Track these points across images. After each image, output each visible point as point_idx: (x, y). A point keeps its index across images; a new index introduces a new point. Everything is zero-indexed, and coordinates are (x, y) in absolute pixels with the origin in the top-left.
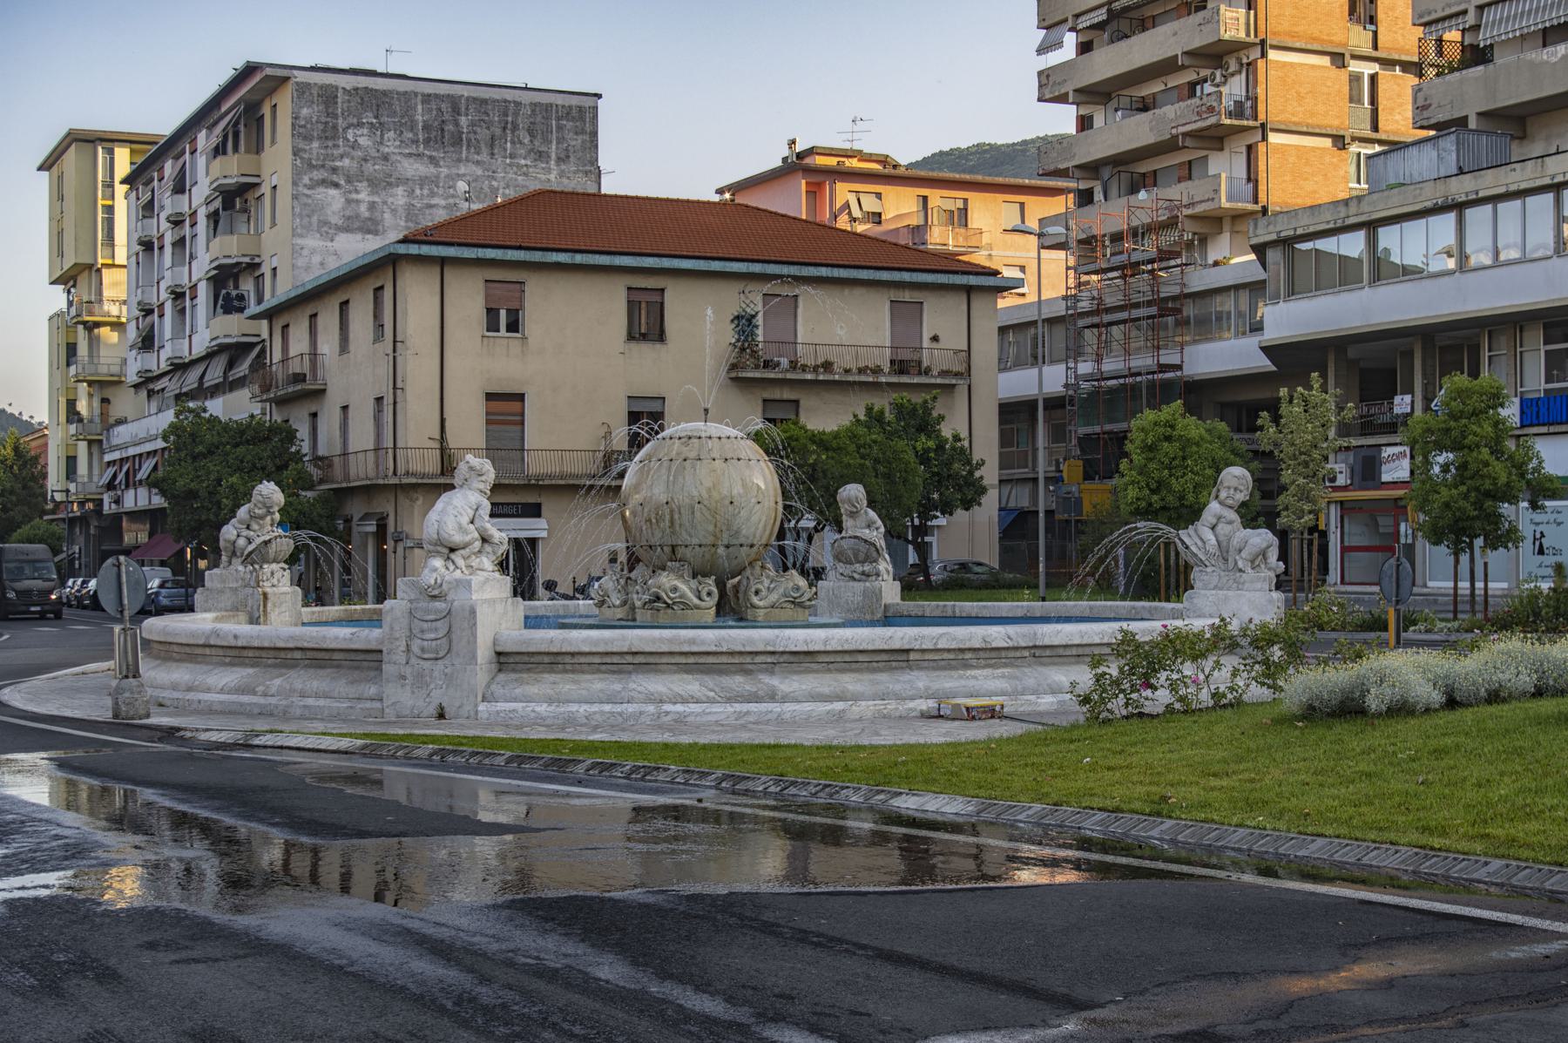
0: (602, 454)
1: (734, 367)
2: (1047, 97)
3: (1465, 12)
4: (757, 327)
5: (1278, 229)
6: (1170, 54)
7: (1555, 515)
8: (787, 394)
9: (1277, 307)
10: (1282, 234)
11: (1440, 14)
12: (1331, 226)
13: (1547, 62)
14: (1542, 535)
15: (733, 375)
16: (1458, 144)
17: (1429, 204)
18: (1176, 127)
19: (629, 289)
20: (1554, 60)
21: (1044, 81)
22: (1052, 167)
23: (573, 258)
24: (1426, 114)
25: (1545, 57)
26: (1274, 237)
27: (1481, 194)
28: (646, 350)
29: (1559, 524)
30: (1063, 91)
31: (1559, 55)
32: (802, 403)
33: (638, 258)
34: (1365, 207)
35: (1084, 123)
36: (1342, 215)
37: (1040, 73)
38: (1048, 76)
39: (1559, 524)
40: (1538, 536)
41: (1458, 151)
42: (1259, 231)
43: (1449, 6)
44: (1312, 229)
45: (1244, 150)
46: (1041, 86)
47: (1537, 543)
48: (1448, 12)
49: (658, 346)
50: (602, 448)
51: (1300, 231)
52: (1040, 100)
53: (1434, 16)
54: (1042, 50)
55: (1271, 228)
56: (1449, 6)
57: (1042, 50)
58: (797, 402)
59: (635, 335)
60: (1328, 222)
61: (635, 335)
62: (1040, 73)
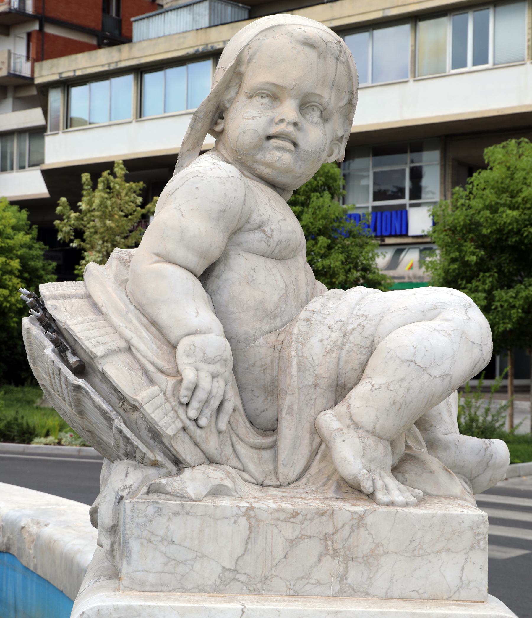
5: (60, 70)
10: (65, 75)
12: (106, 68)
16: (210, 9)
17: (191, 51)
26: (56, 77)
36: (116, 59)
45: (25, 36)
51: (78, 73)
55: (54, 70)
60: (103, 65)
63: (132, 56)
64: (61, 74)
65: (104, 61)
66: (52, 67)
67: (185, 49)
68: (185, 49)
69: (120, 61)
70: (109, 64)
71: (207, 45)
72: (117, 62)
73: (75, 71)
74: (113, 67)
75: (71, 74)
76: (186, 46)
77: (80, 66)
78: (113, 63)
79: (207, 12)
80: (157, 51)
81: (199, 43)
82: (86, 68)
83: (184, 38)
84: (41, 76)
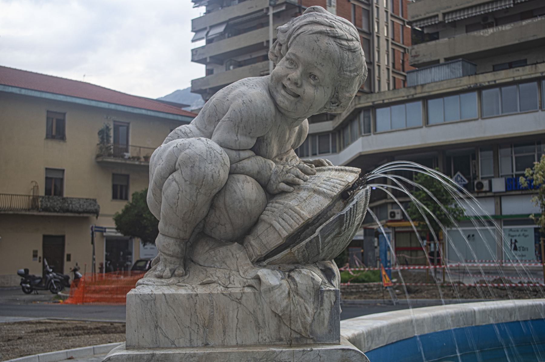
0: (31, 198)
1: (98, 156)
2: (196, 59)
3: (437, 16)
4: (110, 137)
5: (373, 100)
6: (260, 41)
7: (523, 232)
8: (124, 172)
9: (370, 137)
10: (376, 103)
11: (423, 17)
12: (406, 98)
13: (483, 36)
14: (516, 241)
15: (100, 160)
18: (263, 72)
19: (48, 112)
20: (487, 35)
21: (194, 53)
22: (198, 88)
23: (20, 91)
24: (416, 59)
25: (482, 34)
27: (497, 82)
28: (55, 145)
29: (526, 236)
30: (204, 57)
31: (489, 33)
32: (131, 176)
33: (55, 95)
34: (426, 89)
35: (209, 72)
37: (192, 50)
38: (196, 51)
39: (526, 236)
40: (513, 241)
41: (463, 69)
42: (362, 101)
43: (428, 13)
44: (393, 100)
46: (193, 55)
47: (513, 245)
48: (428, 15)
49: (62, 143)
50: (32, 194)
51: (386, 101)
52: (193, 61)
53: (420, 17)
54: (193, 41)
55: (369, 100)
56: (428, 13)
57: (193, 41)
58: (128, 176)
59: (50, 136)
60: (403, 97)
61: (50, 136)
62: (192, 50)
63: (424, 91)
64: (373, 102)
65: (404, 94)
66: (368, 98)
67: (461, 86)
68: (461, 86)
69: (416, 94)
70: (408, 96)
71: (477, 84)
72: (413, 95)
73: (383, 100)
74: (410, 97)
75: (381, 102)
76: (461, 84)
77: (388, 97)
78: (411, 95)
79: (461, 67)
80: (441, 88)
81: (471, 83)
82: (391, 99)
83: (461, 80)
84: (360, 104)
